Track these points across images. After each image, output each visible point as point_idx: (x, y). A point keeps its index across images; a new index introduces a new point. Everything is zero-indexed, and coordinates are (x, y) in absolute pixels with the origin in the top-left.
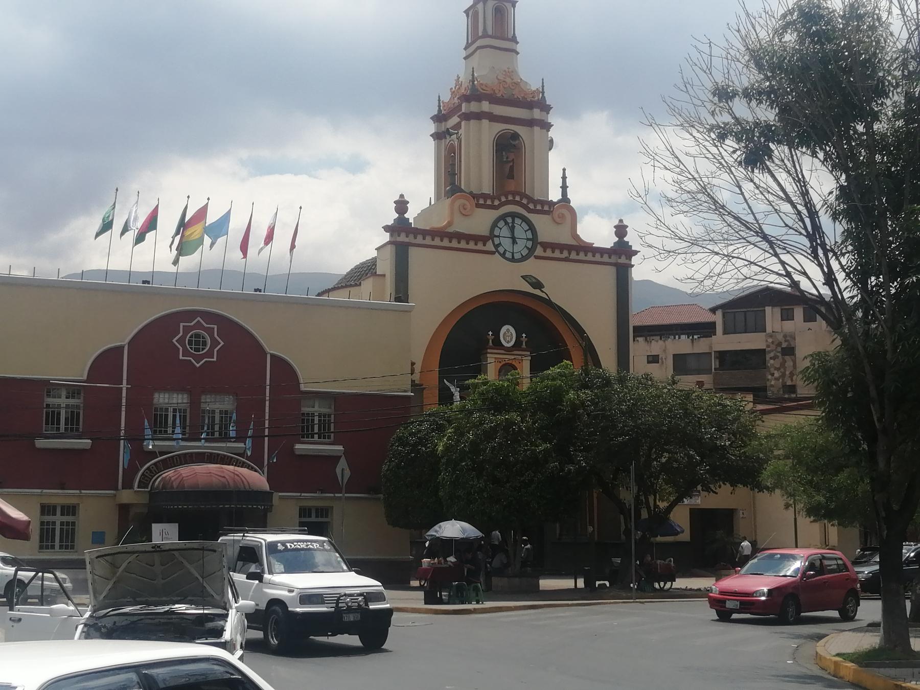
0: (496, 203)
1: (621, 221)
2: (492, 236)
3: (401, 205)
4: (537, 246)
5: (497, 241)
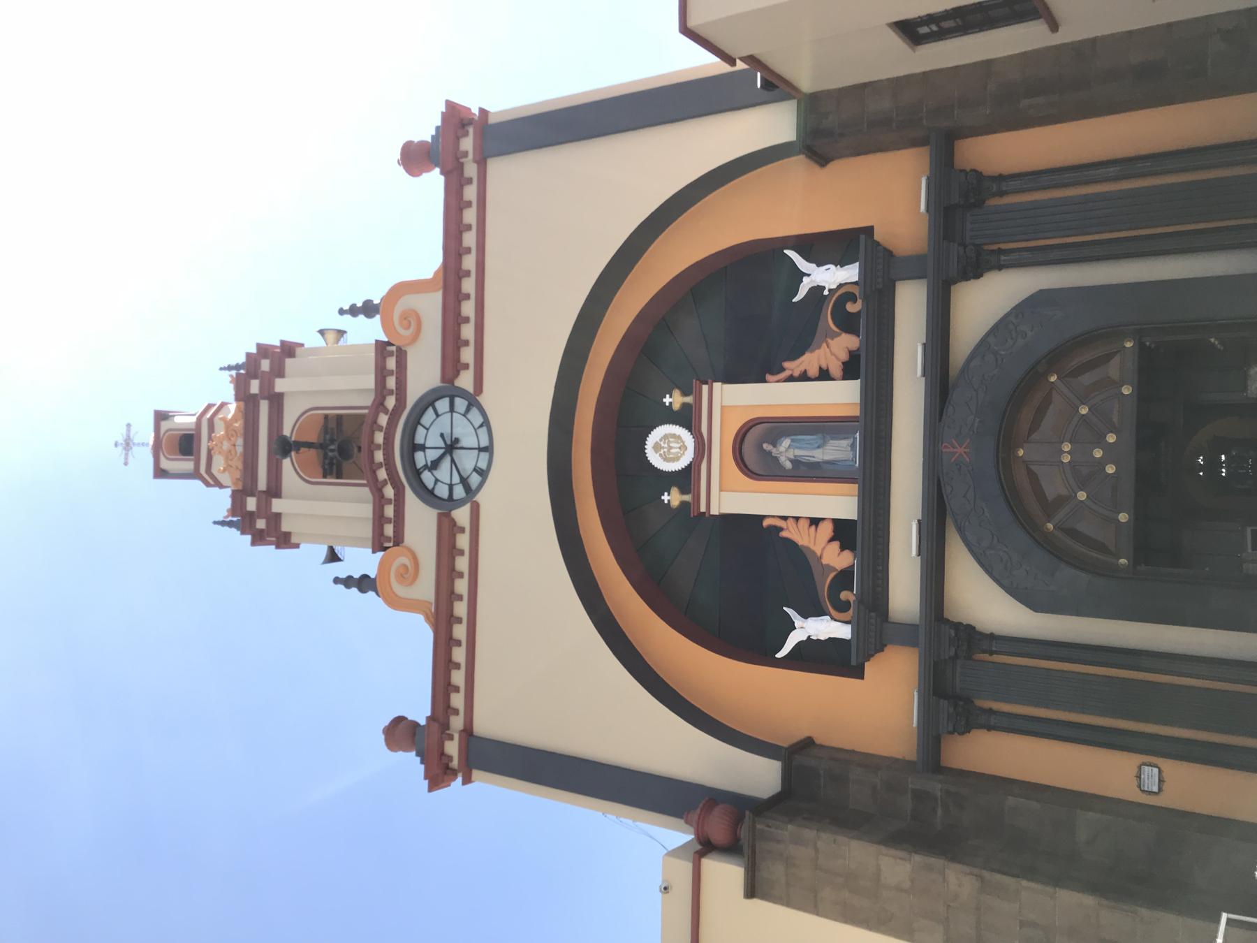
0: (389, 492)
3: (400, 733)
4: (458, 385)
5: (459, 492)
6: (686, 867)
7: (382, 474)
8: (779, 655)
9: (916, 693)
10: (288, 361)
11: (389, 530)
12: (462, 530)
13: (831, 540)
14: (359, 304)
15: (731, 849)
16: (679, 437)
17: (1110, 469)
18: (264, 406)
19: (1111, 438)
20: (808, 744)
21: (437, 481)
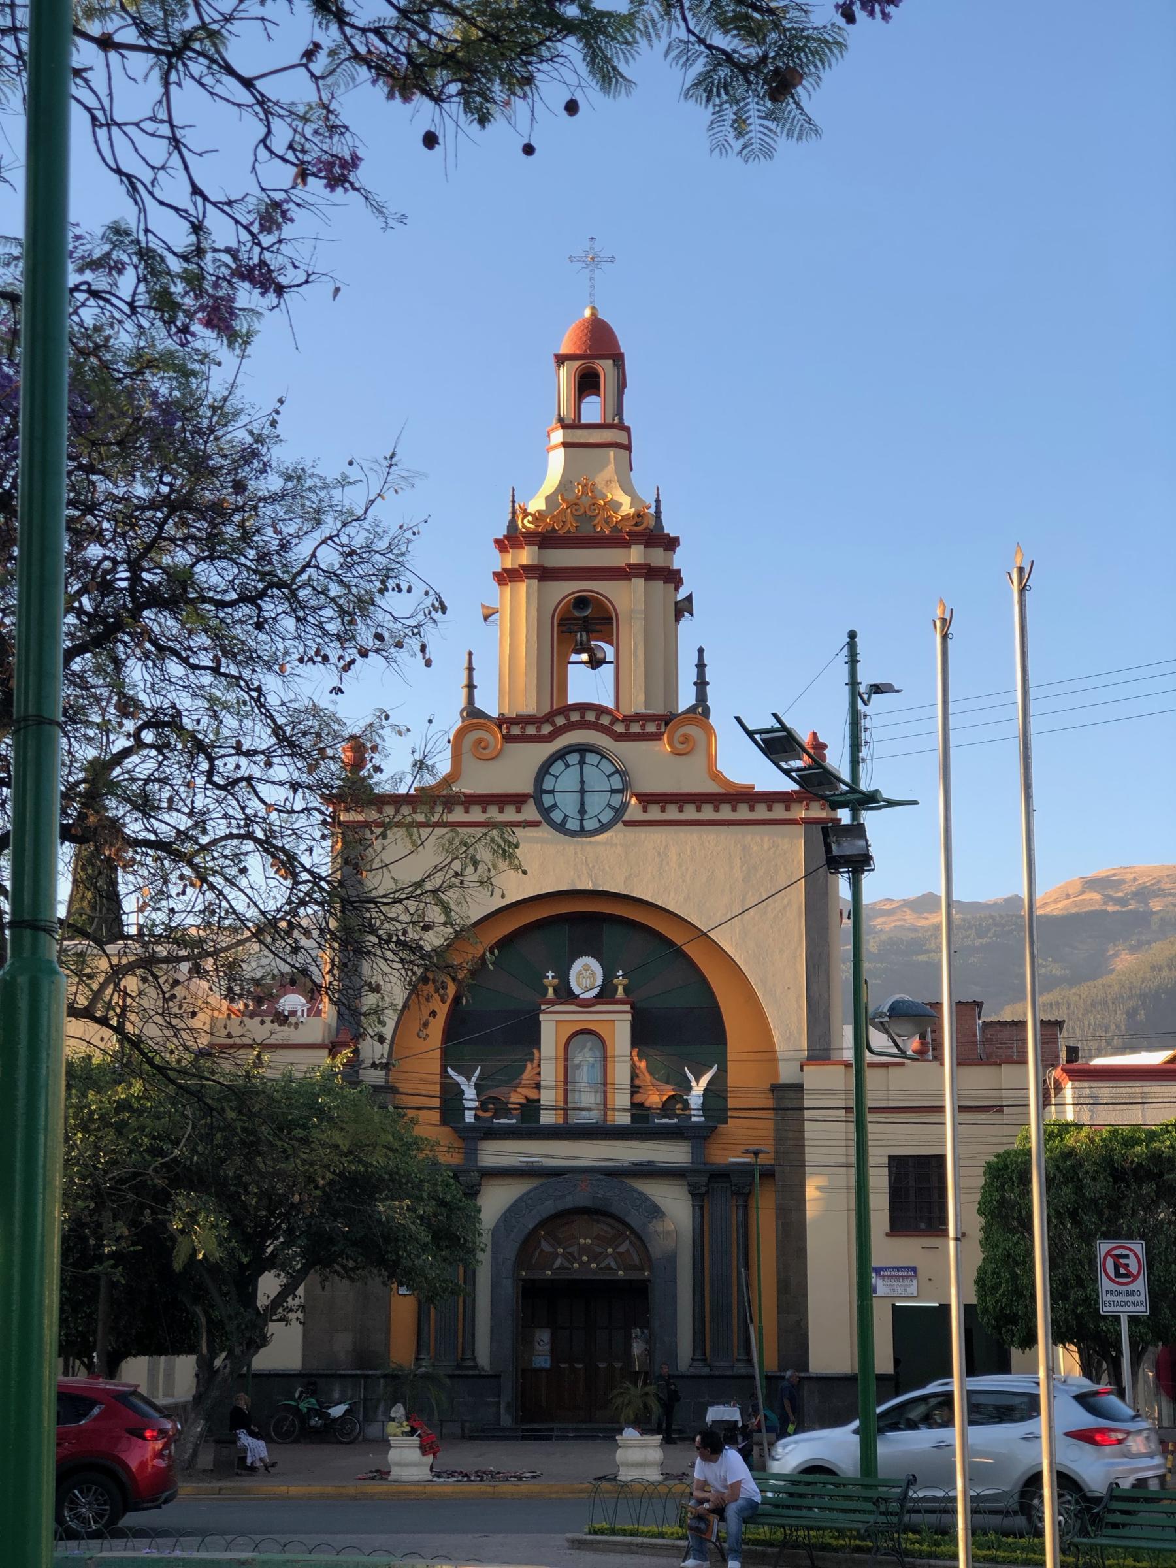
0: (547, 729)
1: (815, 734)
2: (540, 790)
5: (547, 800)
7: (560, 721)
11: (516, 730)
12: (519, 811)
17: (576, 1265)
19: (594, 1265)
21: (557, 777)
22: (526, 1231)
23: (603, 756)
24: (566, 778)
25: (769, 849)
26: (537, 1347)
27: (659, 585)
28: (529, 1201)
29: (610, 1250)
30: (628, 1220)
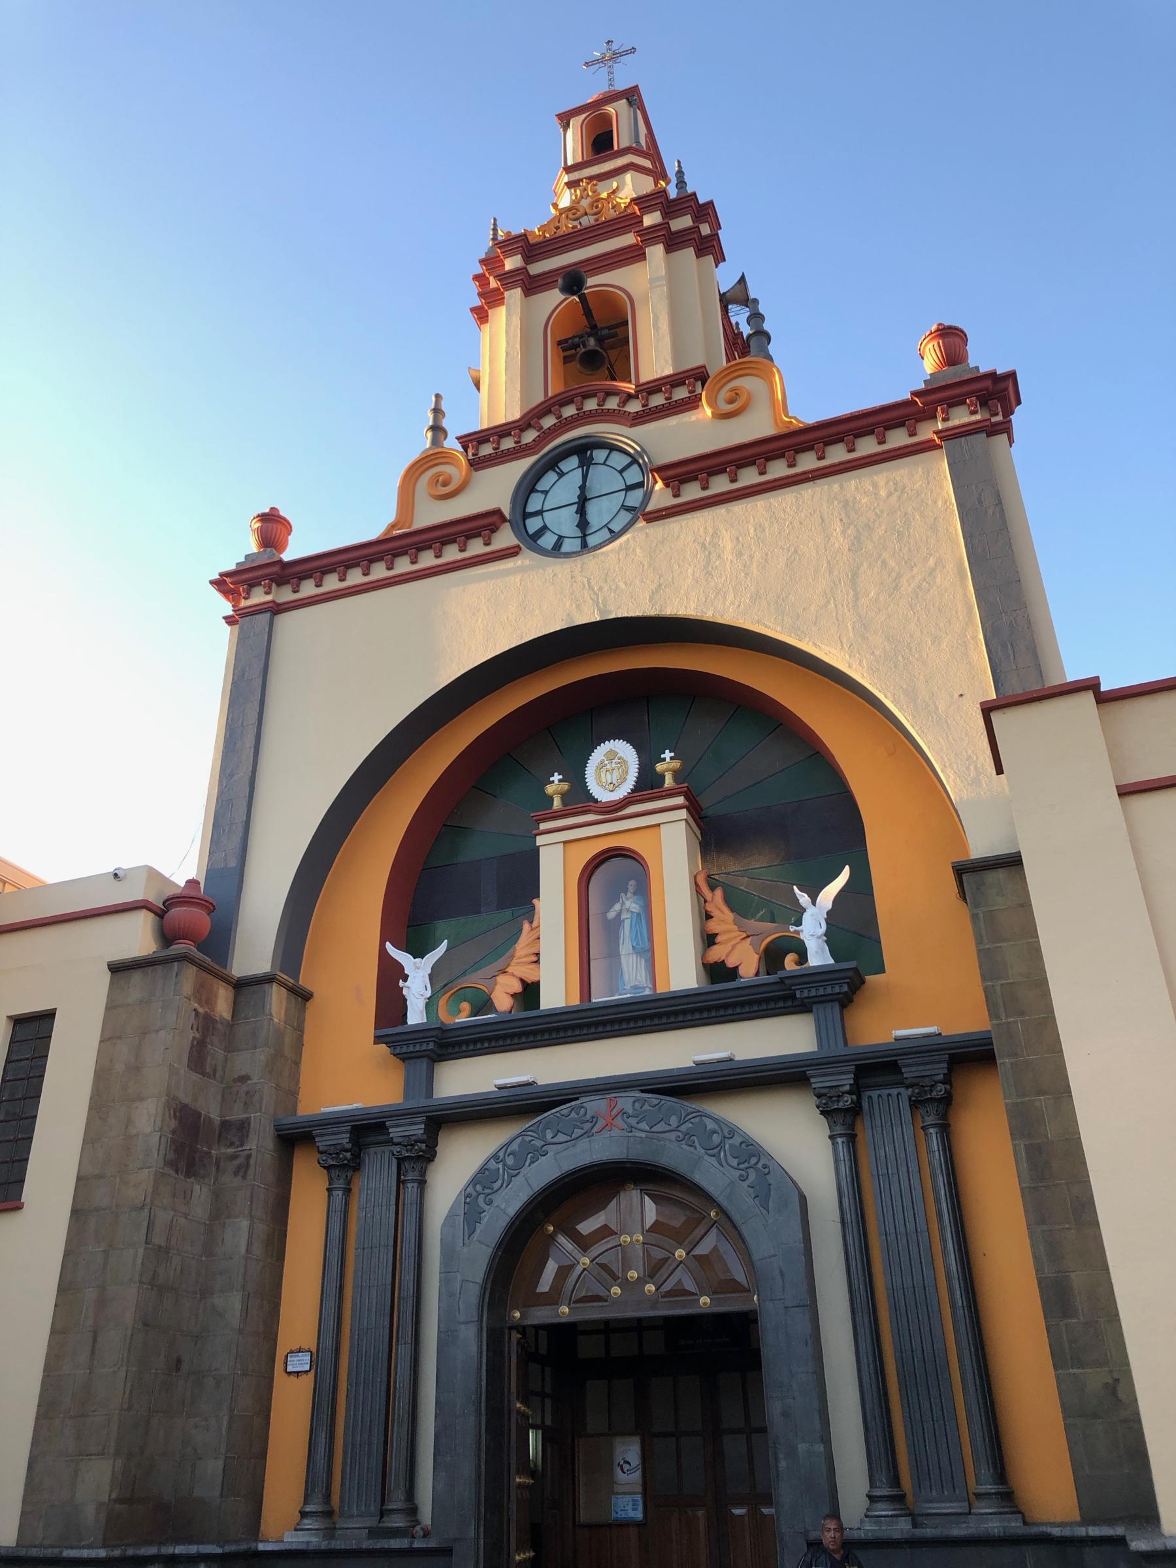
5: (533, 525)
6: (137, 895)
7: (549, 422)
8: (388, 945)
9: (355, 1106)
10: (690, 252)
11: (487, 450)
13: (522, 980)
14: (766, 327)
15: (166, 937)
16: (625, 780)
17: (616, 1290)
18: (629, 239)
20: (302, 996)
21: (546, 493)
22: (502, 1223)
23: (613, 448)
24: (561, 490)
25: (890, 494)
26: (620, 1476)
27: (688, 254)
28: (510, 1161)
29: (680, 1253)
30: (698, 1178)
